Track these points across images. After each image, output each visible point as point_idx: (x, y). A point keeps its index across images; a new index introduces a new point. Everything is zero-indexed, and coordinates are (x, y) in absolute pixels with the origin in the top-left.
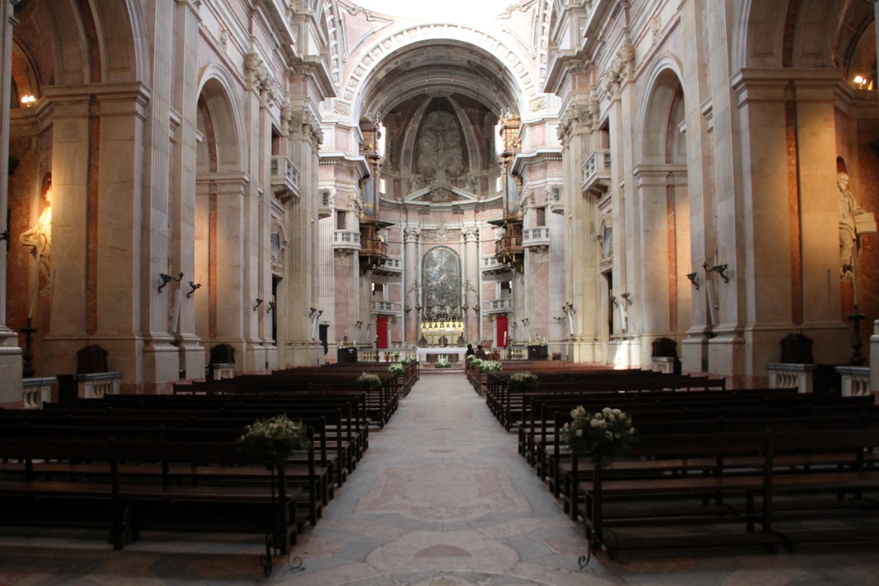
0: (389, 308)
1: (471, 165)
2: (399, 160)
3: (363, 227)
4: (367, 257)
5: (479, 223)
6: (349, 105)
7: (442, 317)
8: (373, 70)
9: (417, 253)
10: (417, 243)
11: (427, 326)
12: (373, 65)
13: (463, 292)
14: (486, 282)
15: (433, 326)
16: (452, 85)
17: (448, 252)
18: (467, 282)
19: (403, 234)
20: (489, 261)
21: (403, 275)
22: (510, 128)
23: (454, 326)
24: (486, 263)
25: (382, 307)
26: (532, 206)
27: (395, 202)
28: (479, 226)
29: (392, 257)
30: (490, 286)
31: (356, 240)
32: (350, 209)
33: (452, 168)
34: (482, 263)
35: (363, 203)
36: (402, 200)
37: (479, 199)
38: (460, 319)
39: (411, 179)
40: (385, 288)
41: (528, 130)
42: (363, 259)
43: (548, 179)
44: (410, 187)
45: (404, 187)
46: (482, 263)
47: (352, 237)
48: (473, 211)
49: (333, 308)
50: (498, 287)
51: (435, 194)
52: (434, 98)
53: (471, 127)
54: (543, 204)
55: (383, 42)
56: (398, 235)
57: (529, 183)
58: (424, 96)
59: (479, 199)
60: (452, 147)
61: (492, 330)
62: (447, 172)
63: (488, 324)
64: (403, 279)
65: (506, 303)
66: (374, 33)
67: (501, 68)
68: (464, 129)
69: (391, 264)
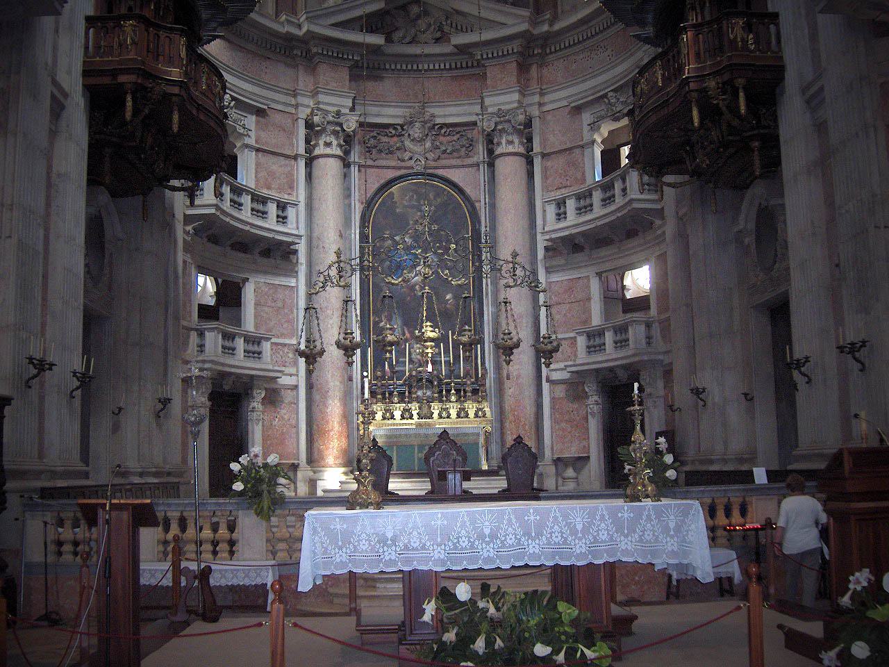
9: (347, 194)
10: (347, 165)
14: (555, 278)
15: (397, 414)
17: (439, 193)
19: (302, 131)
20: (571, 205)
21: (302, 248)
23: (462, 414)
24: (561, 216)
25: (230, 351)
28: (535, 112)
30: (570, 287)
37: (534, 23)
38: (477, 392)
40: (249, 294)
48: (514, 65)
50: (595, 287)
56: (291, 134)
61: (583, 426)
64: (302, 269)
69: (263, 214)
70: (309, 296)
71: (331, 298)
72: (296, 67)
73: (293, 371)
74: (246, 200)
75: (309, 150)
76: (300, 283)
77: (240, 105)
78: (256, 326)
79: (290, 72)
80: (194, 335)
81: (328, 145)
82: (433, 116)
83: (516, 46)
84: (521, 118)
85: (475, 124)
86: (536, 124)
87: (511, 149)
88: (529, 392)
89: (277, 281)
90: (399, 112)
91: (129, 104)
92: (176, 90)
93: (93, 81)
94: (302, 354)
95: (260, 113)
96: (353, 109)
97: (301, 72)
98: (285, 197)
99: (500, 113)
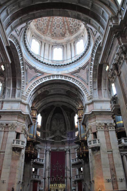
0: (38, 178)
1: (67, 129)
2: (45, 127)
3: (28, 143)
4: (28, 154)
5: (70, 147)
6: (27, 97)
7: (58, 182)
8: (36, 88)
10: (50, 154)
11: (52, 185)
12: (36, 86)
13: (65, 172)
14: (73, 168)
16: (62, 102)
18: (67, 168)
20: (74, 160)
22: (80, 110)
23: (62, 185)
24: (73, 161)
25: (36, 177)
26: (91, 132)
27: (43, 139)
28: (70, 148)
29: (41, 158)
31: (22, 144)
32: (22, 133)
33: (62, 130)
34: (72, 161)
35: (29, 133)
36: (45, 139)
37: (70, 139)
39: (49, 132)
40: (38, 170)
41: (87, 106)
42: (26, 154)
43: (97, 121)
44: (48, 135)
45: (46, 135)
46: (72, 161)
47: (21, 142)
49: (8, 174)
50: (77, 170)
51: (56, 138)
52: (57, 107)
53: (67, 117)
54: (95, 131)
55: (40, 79)
56: (44, 151)
57: (89, 124)
58: (53, 106)
59: (70, 139)
60: (62, 124)
62: (60, 131)
63: (74, 185)
64: (44, 167)
65: (81, 176)
66: (37, 76)
67: (77, 89)
68: (65, 117)
69: (40, 161)
70: (45, 172)
71: (47, 172)
72: (45, 143)
73: (43, 180)
74: (39, 160)
75: (46, 153)
76: (44, 169)
77: (38, 148)
78: (39, 174)
79: (44, 144)
80: (32, 176)
81: (48, 152)
82: (60, 149)
83: (68, 141)
84: (69, 149)
85: (64, 150)
86: (71, 150)
87: (68, 153)
88: (70, 183)
89: (40, 169)
90: (56, 148)
91: (29, 155)
92: (33, 153)
93: (26, 153)
94: (44, 178)
95: (41, 149)
96: (51, 148)
97: (45, 144)
98: (43, 159)
99: (66, 149)
